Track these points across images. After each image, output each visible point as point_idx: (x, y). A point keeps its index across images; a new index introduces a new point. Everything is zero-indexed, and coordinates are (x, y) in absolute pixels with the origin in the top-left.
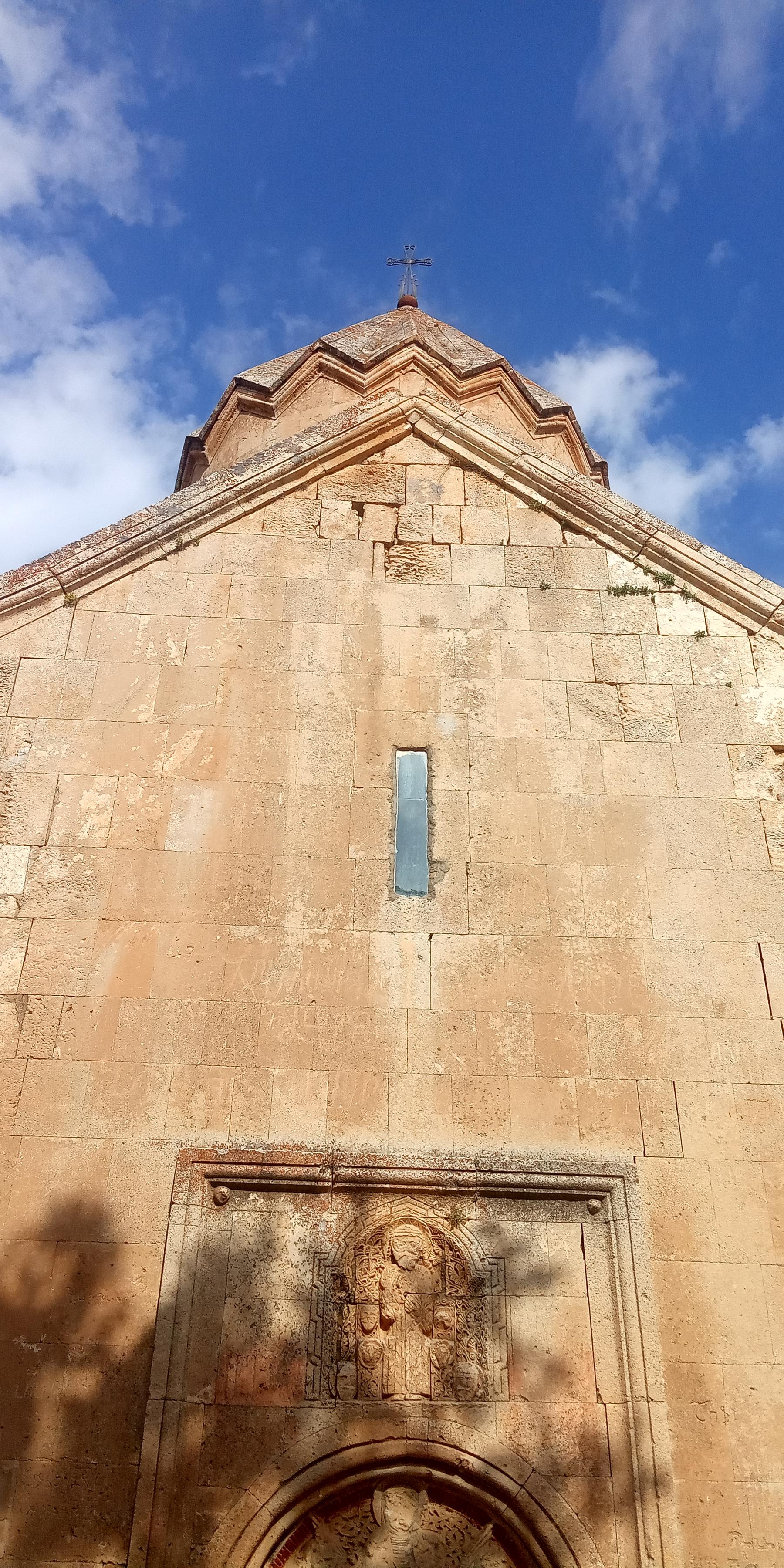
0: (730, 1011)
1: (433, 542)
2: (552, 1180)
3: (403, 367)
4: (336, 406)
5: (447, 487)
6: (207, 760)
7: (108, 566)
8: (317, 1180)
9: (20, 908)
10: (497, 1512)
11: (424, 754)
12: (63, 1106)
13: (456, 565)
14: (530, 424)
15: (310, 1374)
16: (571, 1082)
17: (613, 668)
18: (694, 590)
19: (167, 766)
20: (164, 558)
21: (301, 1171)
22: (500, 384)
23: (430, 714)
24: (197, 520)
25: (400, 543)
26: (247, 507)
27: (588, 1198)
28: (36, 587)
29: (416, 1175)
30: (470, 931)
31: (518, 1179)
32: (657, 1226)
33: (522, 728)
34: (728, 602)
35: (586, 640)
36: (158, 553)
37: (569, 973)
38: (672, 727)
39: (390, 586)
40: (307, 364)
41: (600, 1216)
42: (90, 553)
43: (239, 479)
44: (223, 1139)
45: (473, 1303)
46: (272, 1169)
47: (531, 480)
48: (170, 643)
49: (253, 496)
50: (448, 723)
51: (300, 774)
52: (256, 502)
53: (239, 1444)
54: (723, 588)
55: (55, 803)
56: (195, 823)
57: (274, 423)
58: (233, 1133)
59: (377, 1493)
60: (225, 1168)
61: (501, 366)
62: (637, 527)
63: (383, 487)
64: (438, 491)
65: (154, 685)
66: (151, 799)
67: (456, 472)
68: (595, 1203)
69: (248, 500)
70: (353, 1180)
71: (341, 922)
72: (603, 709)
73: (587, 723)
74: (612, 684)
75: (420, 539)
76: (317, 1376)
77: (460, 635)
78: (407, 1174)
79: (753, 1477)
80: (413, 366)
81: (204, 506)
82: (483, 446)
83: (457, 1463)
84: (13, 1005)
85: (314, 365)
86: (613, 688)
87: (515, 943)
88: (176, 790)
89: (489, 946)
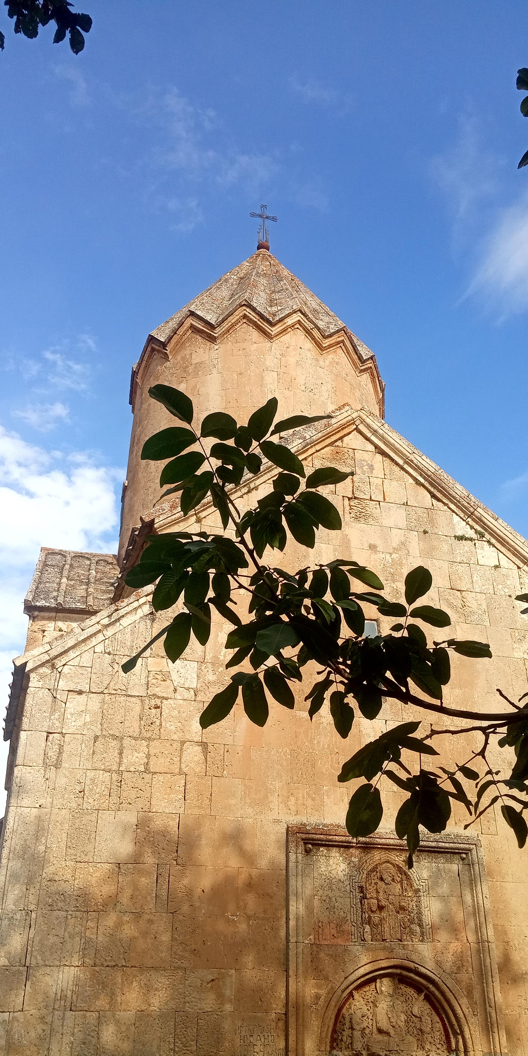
1: (371, 500)
2: (447, 845)
4: (255, 345)
5: (376, 466)
8: (350, 843)
9: (196, 695)
10: (428, 989)
11: (375, 622)
12: (233, 802)
13: (383, 514)
14: (357, 367)
15: (353, 930)
17: (458, 582)
18: (493, 541)
20: (242, 497)
22: (343, 341)
25: (355, 498)
27: (461, 853)
31: (433, 844)
34: (509, 550)
35: (446, 565)
37: (447, 744)
38: (486, 617)
39: (353, 524)
40: (237, 313)
41: (466, 862)
46: (331, 837)
47: (417, 468)
53: (326, 961)
54: (508, 543)
57: (216, 347)
58: (308, 818)
59: (378, 981)
60: (310, 836)
61: (344, 330)
62: (468, 503)
63: (344, 462)
64: (371, 468)
67: (379, 457)
68: (464, 856)
70: (365, 843)
72: (455, 604)
74: (458, 590)
75: (365, 497)
76: (356, 931)
77: (388, 556)
80: (298, 326)
82: (394, 446)
83: (414, 968)
84: (200, 748)
85: (241, 314)
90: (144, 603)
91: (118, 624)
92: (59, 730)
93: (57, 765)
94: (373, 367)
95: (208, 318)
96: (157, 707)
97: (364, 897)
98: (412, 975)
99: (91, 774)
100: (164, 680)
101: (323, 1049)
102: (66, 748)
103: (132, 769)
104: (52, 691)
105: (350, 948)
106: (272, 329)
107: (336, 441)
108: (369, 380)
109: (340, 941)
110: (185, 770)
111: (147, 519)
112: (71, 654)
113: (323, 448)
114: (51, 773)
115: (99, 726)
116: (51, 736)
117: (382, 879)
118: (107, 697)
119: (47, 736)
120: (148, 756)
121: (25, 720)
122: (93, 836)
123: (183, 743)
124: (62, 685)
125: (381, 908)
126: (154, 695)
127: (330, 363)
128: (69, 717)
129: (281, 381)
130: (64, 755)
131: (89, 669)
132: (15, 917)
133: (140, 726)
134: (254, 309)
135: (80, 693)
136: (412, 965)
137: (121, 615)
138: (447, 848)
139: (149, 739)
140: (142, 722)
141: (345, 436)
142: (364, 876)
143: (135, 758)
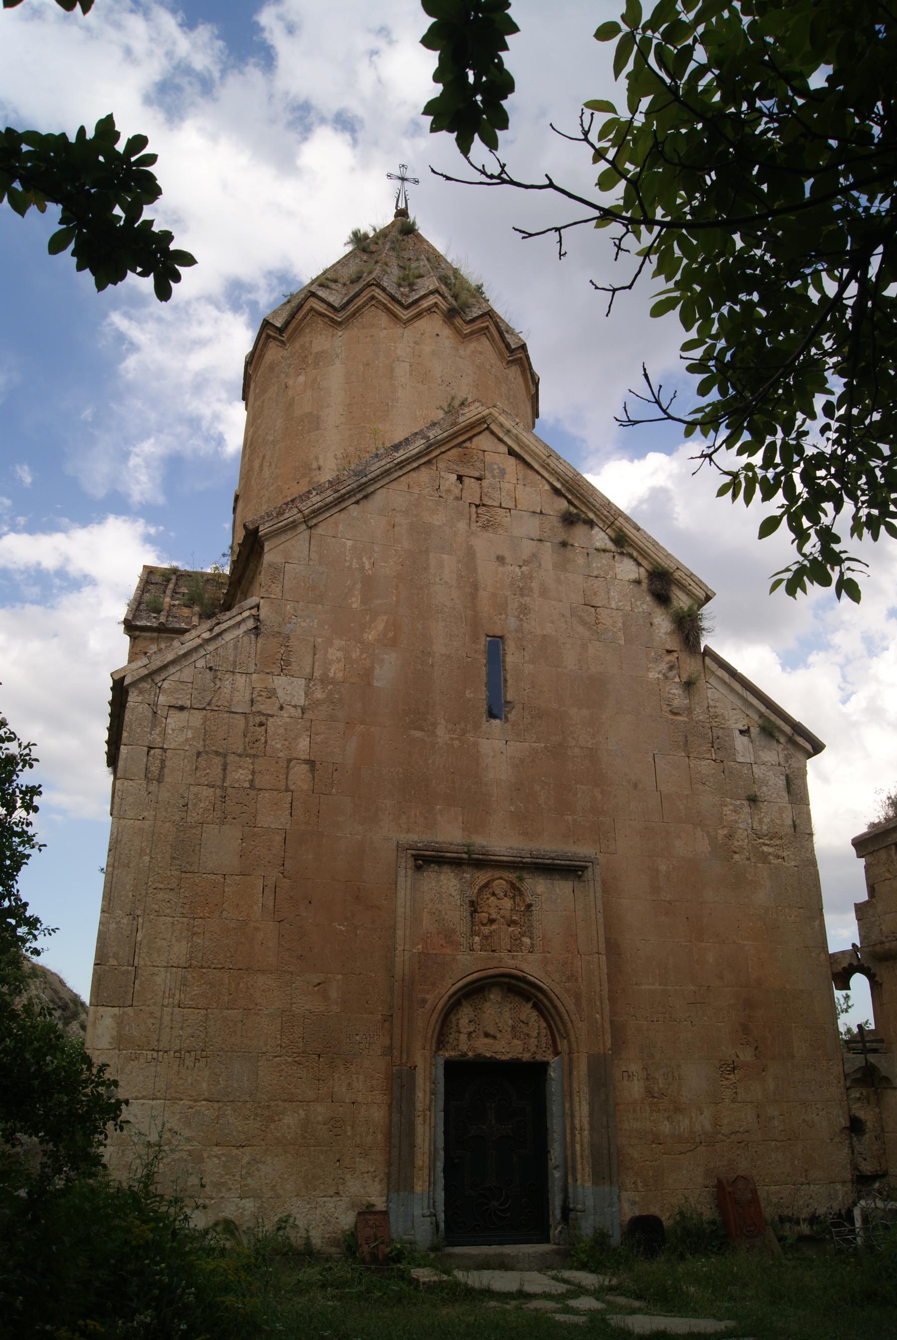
1: (500, 507)
2: (563, 862)
3: (429, 310)
4: (384, 331)
5: (508, 470)
6: (390, 635)
7: (327, 507)
9: (303, 713)
10: (536, 997)
16: (570, 818)
19: (370, 636)
21: (455, 855)
22: (487, 328)
23: (503, 616)
24: (375, 480)
25: (484, 505)
26: (400, 473)
28: (291, 519)
29: (505, 859)
30: (525, 741)
31: (549, 861)
32: (604, 883)
36: (354, 499)
38: (620, 634)
40: (364, 294)
42: (319, 498)
43: (397, 455)
44: (416, 838)
45: (527, 914)
48: (364, 559)
49: (404, 466)
50: (512, 623)
51: (439, 647)
52: (405, 470)
54: (649, 556)
55: (315, 654)
56: (387, 671)
57: (340, 333)
64: (503, 472)
65: (359, 586)
66: (364, 656)
67: (512, 460)
68: (580, 873)
69: (401, 469)
71: (464, 732)
73: (580, 629)
77: (517, 569)
78: (501, 858)
79: (636, 984)
81: (378, 472)
82: (528, 446)
86: (593, 609)
87: (546, 747)
88: (377, 651)
89: (534, 749)
90: (248, 617)
91: (220, 638)
92: (161, 745)
93: (160, 780)
94: (524, 358)
95: (331, 299)
96: (261, 724)
97: (475, 911)
98: (521, 984)
99: (194, 789)
100: (270, 698)
101: (428, 1047)
103: (236, 785)
104: (153, 706)
105: (458, 957)
106: (405, 313)
107: (464, 441)
108: (519, 372)
109: (448, 951)
110: (292, 787)
111: (251, 527)
112: (172, 670)
113: (449, 450)
114: (153, 787)
115: (202, 742)
116: (152, 752)
117: (494, 894)
118: (209, 714)
119: (149, 751)
120: (253, 773)
121: (125, 734)
122: (198, 847)
123: (289, 761)
125: (492, 921)
126: (258, 712)
127: (472, 352)
128: (170, 732)
129: (414, 373)
131: (190, 685)
132: (122, 921)
133: (244, 743)
134: (384, 290)
135: (182, 708)
136: (520, 974)
137: (223, 628)
138: (563, 865)
139: (254, 756)
140: (247, 739)
141: (475, 435)
142: (476, 891)
143: (240, 775)
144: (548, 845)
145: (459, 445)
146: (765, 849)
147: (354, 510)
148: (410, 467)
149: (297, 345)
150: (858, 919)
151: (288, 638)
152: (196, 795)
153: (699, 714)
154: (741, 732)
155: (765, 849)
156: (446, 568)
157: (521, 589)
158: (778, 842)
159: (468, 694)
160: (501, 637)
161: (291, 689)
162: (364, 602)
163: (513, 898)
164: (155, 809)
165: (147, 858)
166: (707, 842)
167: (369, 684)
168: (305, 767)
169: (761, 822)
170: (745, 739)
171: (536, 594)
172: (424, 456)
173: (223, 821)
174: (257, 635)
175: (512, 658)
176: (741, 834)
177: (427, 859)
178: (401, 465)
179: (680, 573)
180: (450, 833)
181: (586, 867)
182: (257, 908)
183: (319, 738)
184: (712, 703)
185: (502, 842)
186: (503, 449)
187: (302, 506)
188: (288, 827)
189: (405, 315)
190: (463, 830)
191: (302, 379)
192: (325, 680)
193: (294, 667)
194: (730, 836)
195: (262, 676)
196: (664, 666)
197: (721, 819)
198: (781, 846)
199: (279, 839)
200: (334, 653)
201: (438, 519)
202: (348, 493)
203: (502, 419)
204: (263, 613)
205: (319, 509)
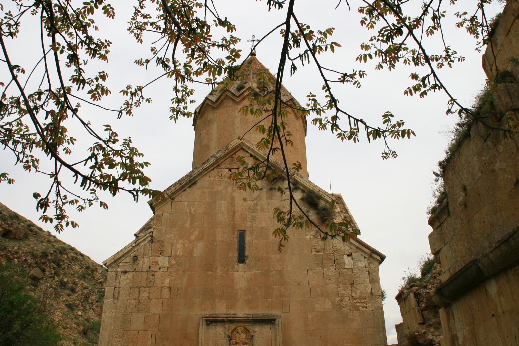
0: (301, 284)
19: (193, 237)
26: (206, 172)
30: (252, 271)
33: (264, 224)
36: (188, 186)
42: (174, 188)
44: (208, 313)
48: (192, 208)
50: (249, 224)
51: (219, 238)
52: (208, 171)
56: (199, 250)
65: (189, 219)
70: (231, 320)
71: (228, 270)
87: (261, 272)
96: (153, 275)
97: (231, 339)
99: (129, 301)
102: (121, 292)
104: (116, 272)
107: (233, 155)
114: (116, 301)
117: (238, 333)
118: (135, 273)
120: (149, 293)
123: (162, 287)
124: (119, 269)
130: (120, 295)
134: (230, 92)
141: (237, 152)
143: (144, 295)
144: (261, 312)
145: (231, 157)
146: (358, 304)
147: (188, 190)
148: (210, 170)
149: (204, 118)
150: (397, 331)
151: (163, 242)
152: (130, 303)
153: (329, 251)
154: (348, 255)
155: (358, 304)
156: (223, 206)
157: (253, 210)
158: (364, 301)
159: (230, 255)
160: (244, 231)
161: (163, 261)
162: (191, 224)
163: (246, 333)
164: (116, 309)
165: (113, 327)
166: (330, 303)
167: (192, 256)
168: (168, 290)
169: (356, 293)
170: (350, 258)
171: (259, 211)
172: (215, 164)
173: (138, 311)
174: (152, 242)
175: (248, 238)
176: (346, 299)
177: (211, 321)
178: (206, 169)
179: (320, 192)
180: (221, 310)
181: (275, 319)
182: (149, 343)
183: (173, 278)
184: (334, 245)
185: (241, 313)
186: (248, 155)
187: (168, 192)
188: (161, 312)
189: (238, 100)
190: (226, 308)
191: (204, 131)
192: (176, 256)
193: (165, 253)
194: (341, 301)
195: (153, 257)
196: (313, 232)
197: (338, 294)
198: (366, 302)
199: (157, 317)
200: (179, 246)
201: (221, 188)
202: (185, 184)
203: (246, 143)
204: (154, 234)
205: (174, 192)
